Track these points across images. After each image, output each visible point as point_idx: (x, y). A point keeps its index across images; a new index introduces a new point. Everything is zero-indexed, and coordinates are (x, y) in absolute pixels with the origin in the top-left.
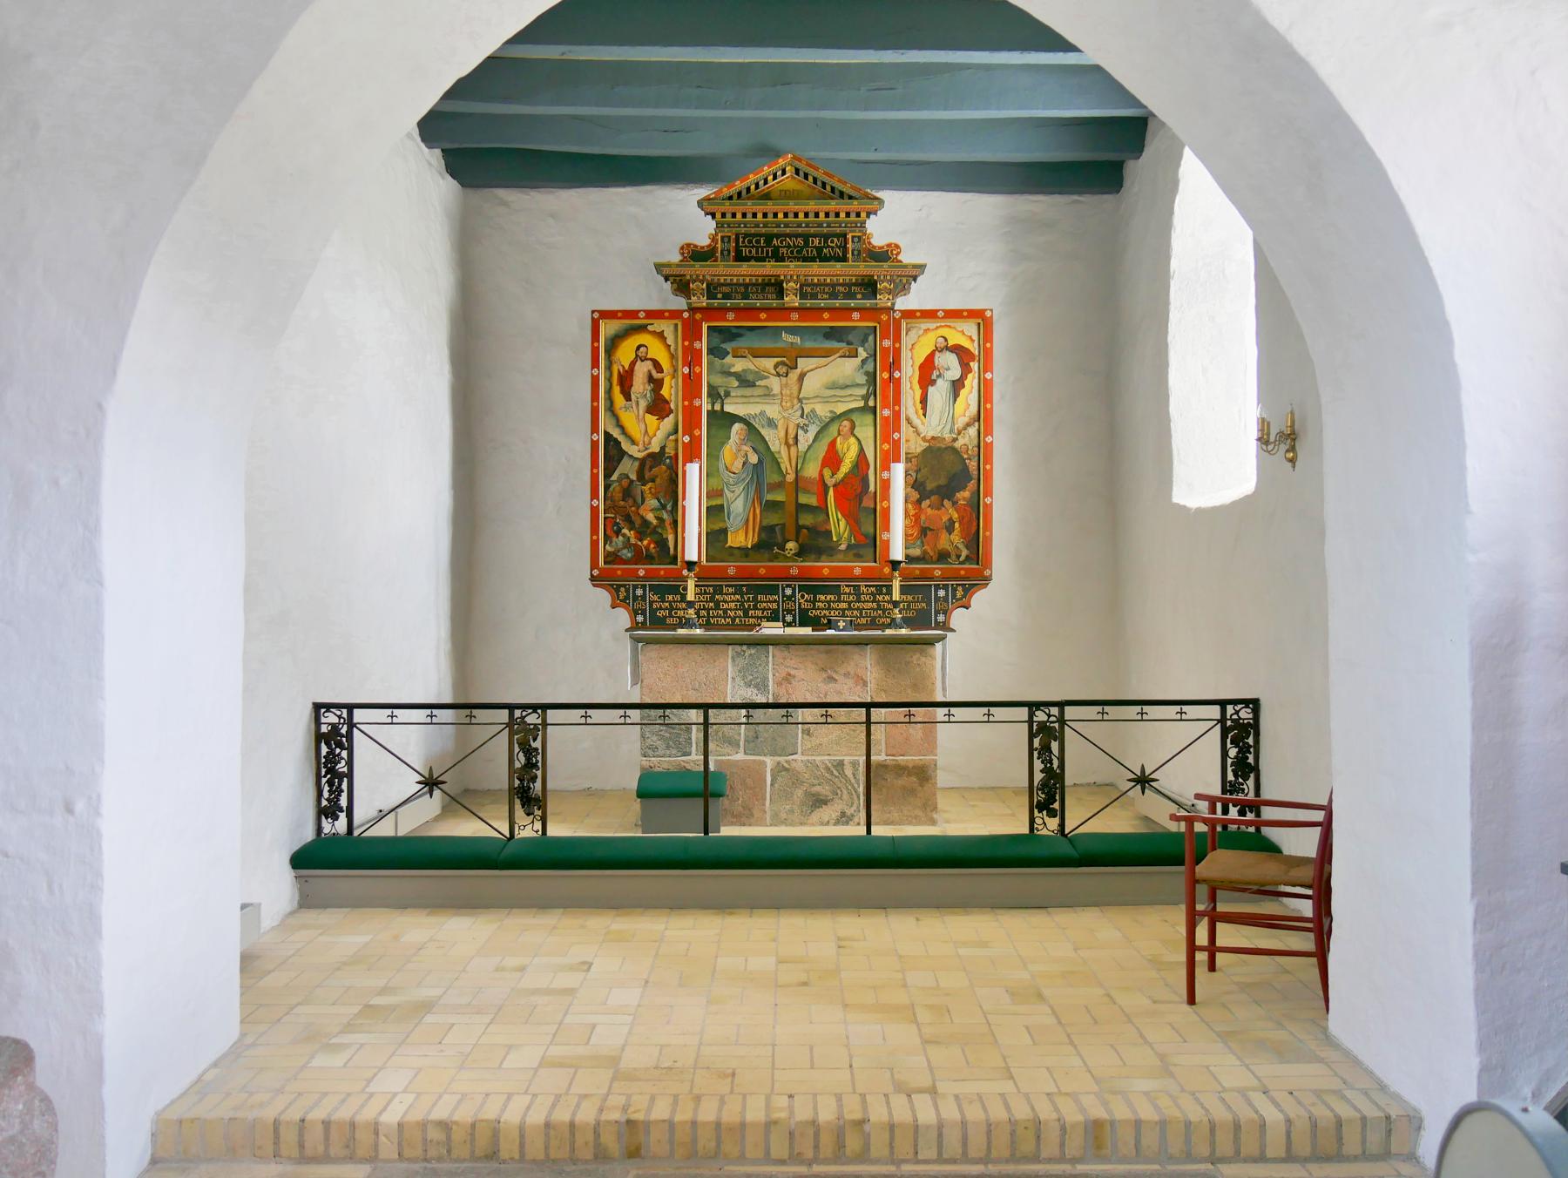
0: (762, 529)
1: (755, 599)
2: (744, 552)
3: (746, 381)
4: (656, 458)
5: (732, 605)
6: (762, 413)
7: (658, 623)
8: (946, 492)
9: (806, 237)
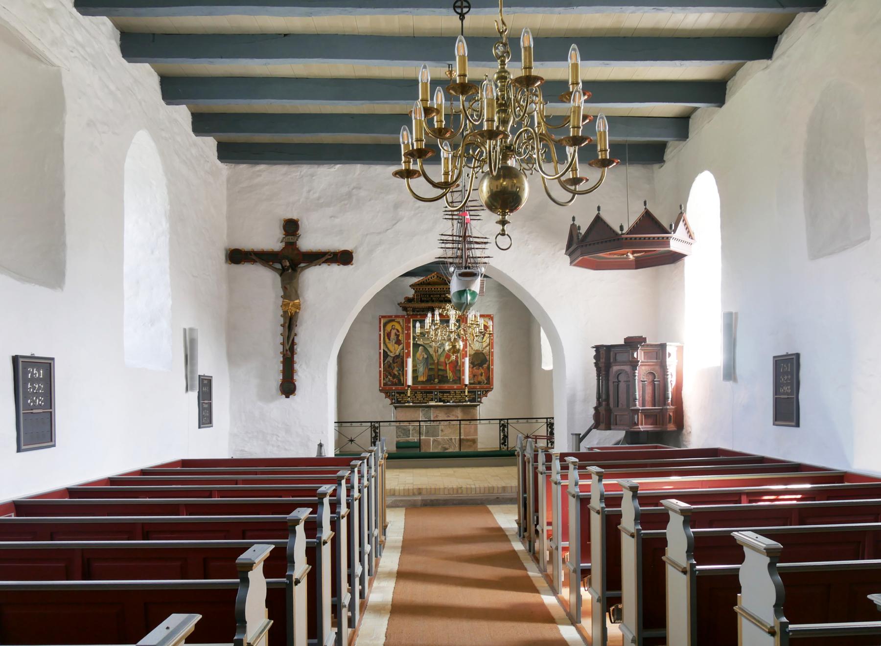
0: (428, 376)
2: (423, 382)
4: (398, 356)
7: (399, 402)
8: (480, 365)
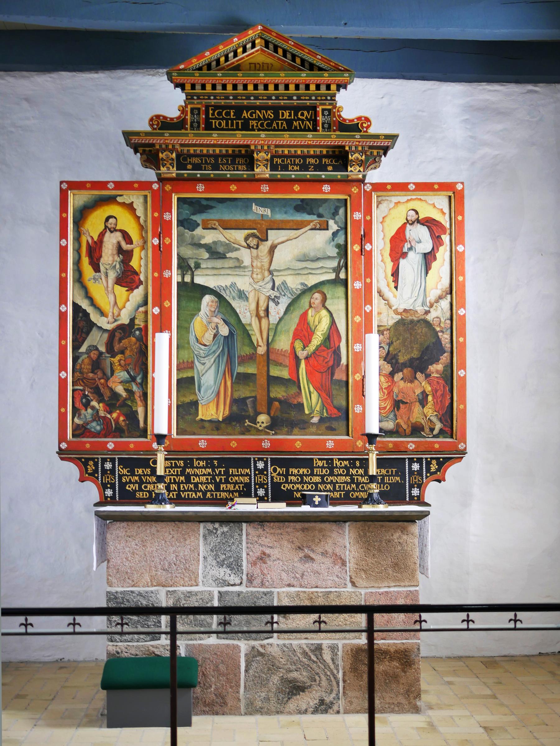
0: (234, 401)
1: (227, 473)
2: (216, 426)
3: (216, 253)
4: (126, 330)
5: (203, 479)
6: (233, 285)
7: (127, 497)
8: (419, 365)
9: (276, 109)
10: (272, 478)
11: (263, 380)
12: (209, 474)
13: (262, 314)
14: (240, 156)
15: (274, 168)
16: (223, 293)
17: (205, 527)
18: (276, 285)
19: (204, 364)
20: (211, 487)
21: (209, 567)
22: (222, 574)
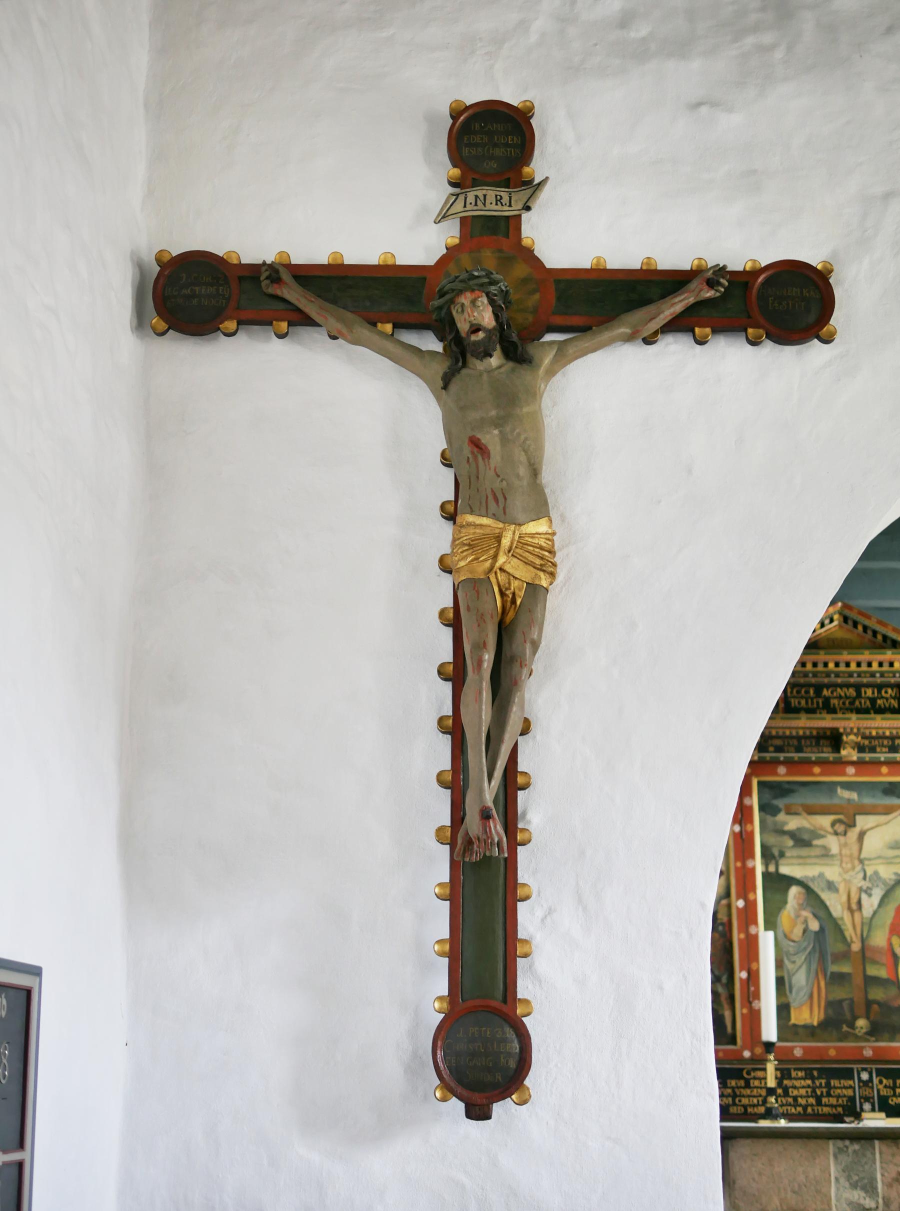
0: (830, 1004)
1: (828, 1085)
2: (810, 1031)
3: (802, 840)
5: (803, 1092)
6: (821, 875)
9: (858, 687)
10: (878, 1091)
11: (859, 980)
12: (809, 1087)
13: (854, 906)
14: (825, 737)
15: (861, 749)
16: (811, 884)
17: (834, 1145)
18: (868, 874)
19: (794, 962)
20: (812, 1101)
21: (842, 1189)
22: (856, 1197)
